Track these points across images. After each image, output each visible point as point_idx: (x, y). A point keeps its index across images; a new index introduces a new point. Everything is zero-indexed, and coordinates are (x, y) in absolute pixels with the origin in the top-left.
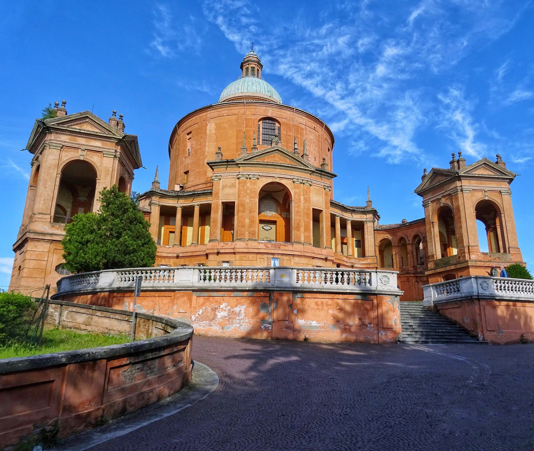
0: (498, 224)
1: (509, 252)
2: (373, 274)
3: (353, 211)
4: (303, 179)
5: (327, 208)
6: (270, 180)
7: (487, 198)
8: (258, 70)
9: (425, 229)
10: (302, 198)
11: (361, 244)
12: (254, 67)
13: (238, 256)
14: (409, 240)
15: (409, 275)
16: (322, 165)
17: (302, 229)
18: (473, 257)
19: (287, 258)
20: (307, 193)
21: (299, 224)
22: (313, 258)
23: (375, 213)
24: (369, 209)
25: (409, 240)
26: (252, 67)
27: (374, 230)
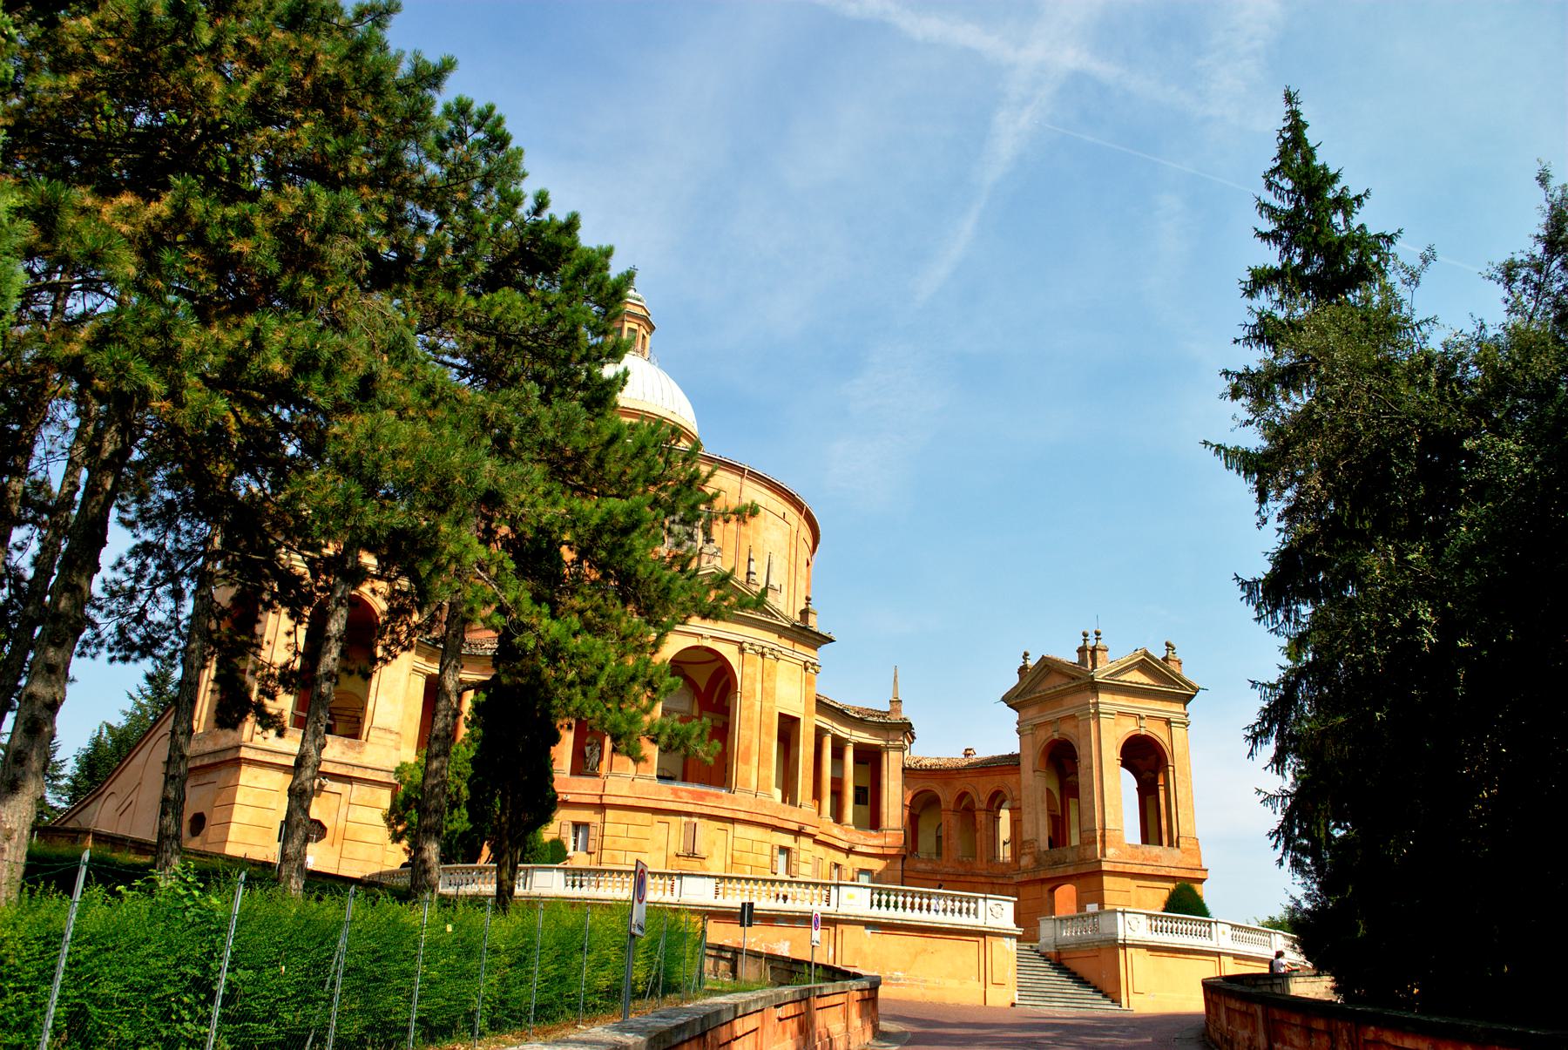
0: (1161, 782)
1: (1178, 846)
2: (980, 901)
3: (859, 722)
4: (764, 644)
5: (807, 713)
6: (692, 642)
7: (1143, 732)
8: (644, 337)
9: (1019, 783)
10: (758, 687)
11: (869, 796)
12: (635, 331)
13: (610, 814)
14: (981, 801)
15: (976, 879)
16: (805, 613)
17: (755, 759)
18: (1110, 852)
19: (720, 825)
20: (766, 676)
21: (748, 749)
22: (775, 828)
23: (906, 729)
24: (894, 719)
25: (981, 801)
26: (630, 329)
27: (904, 769)
